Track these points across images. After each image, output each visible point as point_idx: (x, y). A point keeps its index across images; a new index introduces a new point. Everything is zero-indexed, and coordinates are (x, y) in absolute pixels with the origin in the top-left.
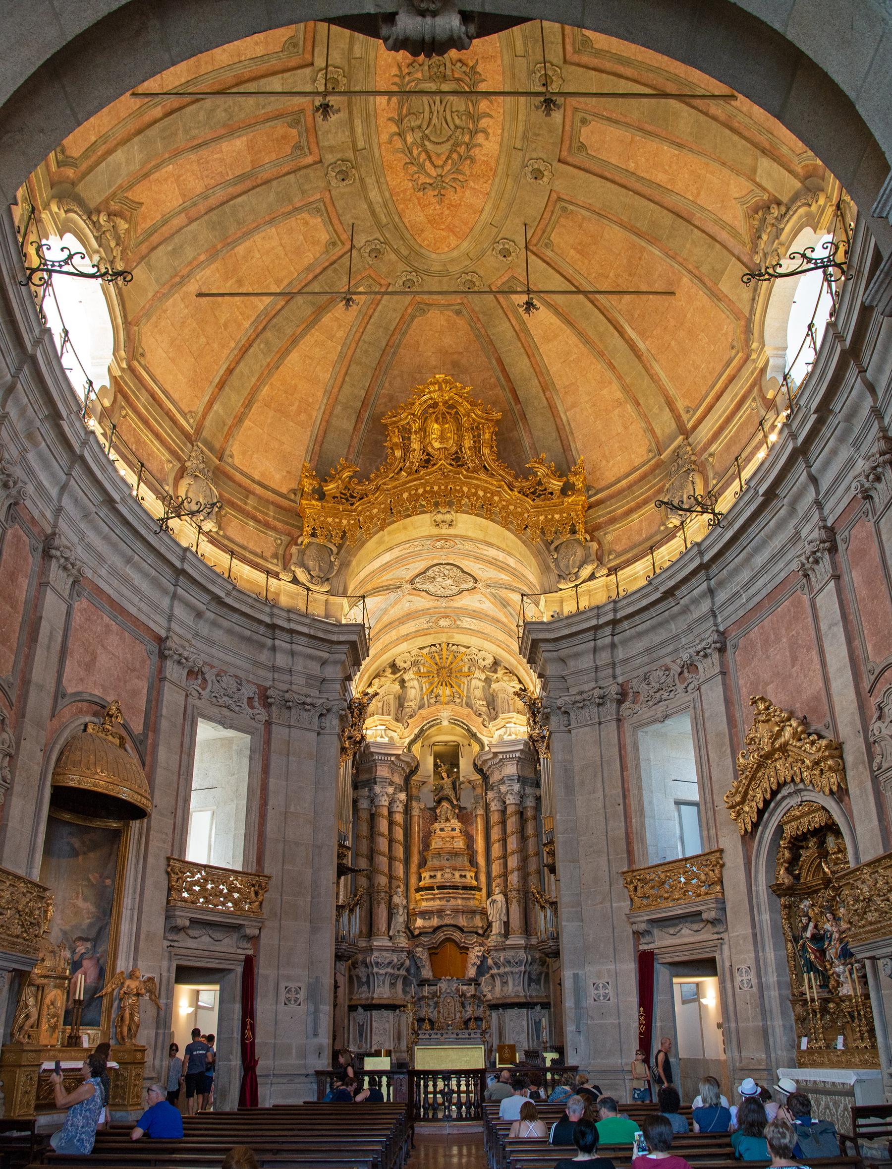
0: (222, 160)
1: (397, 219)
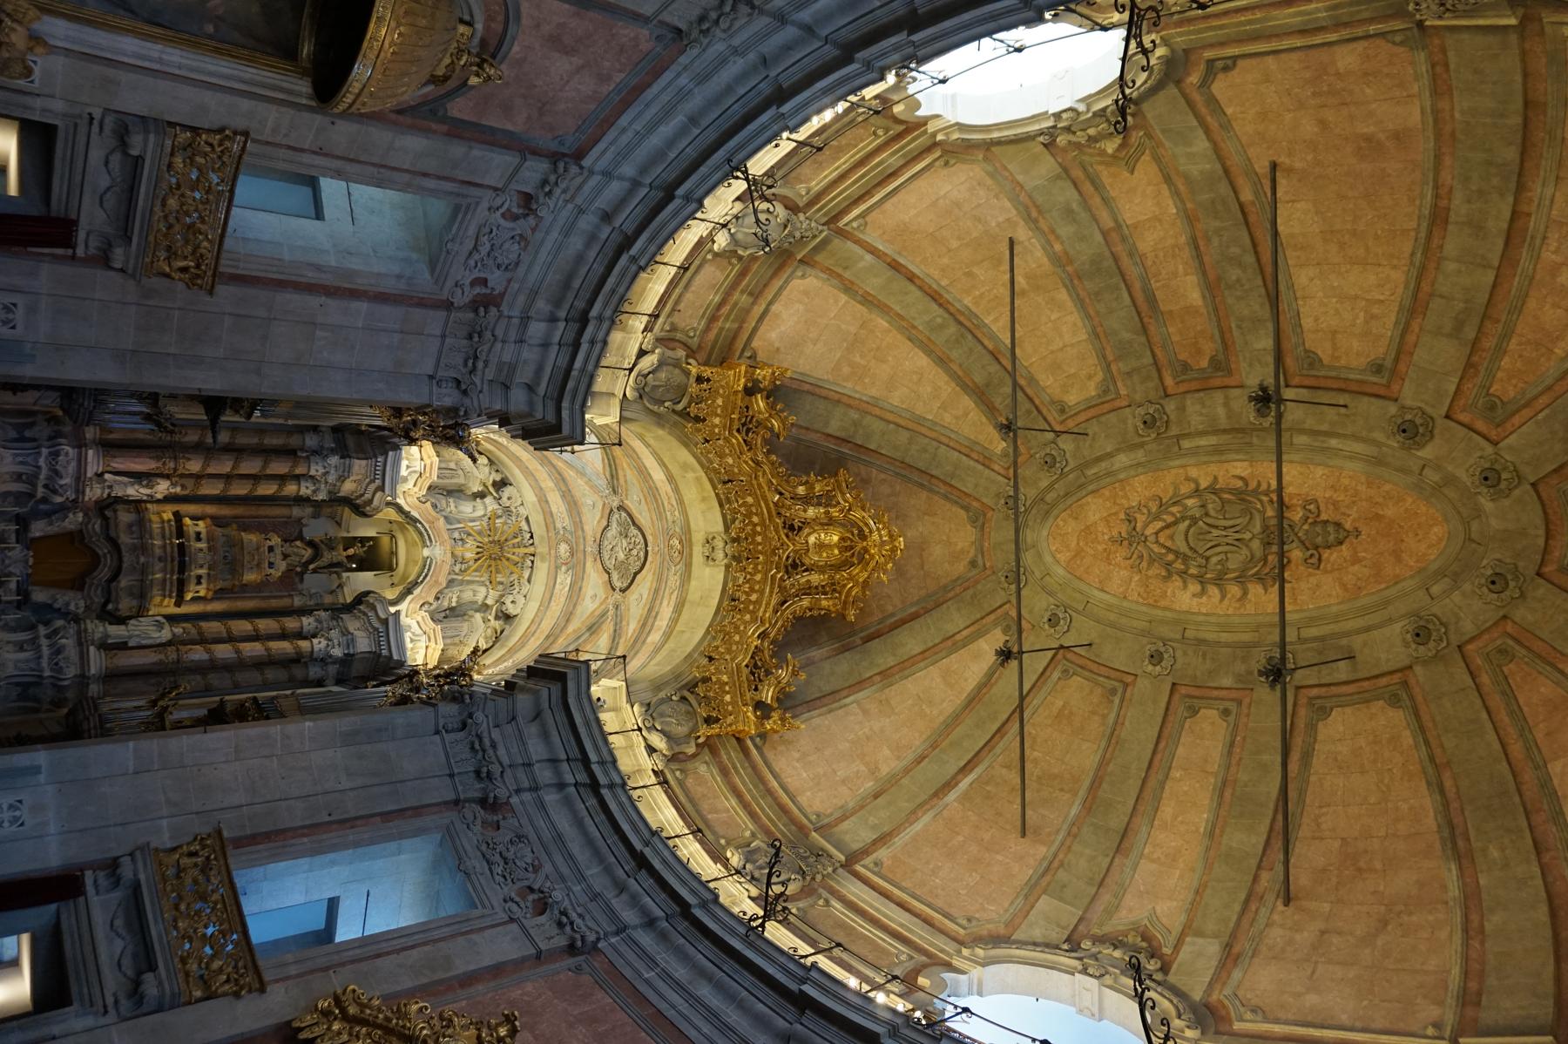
0: (1175, 274)
1: (1091, 488)
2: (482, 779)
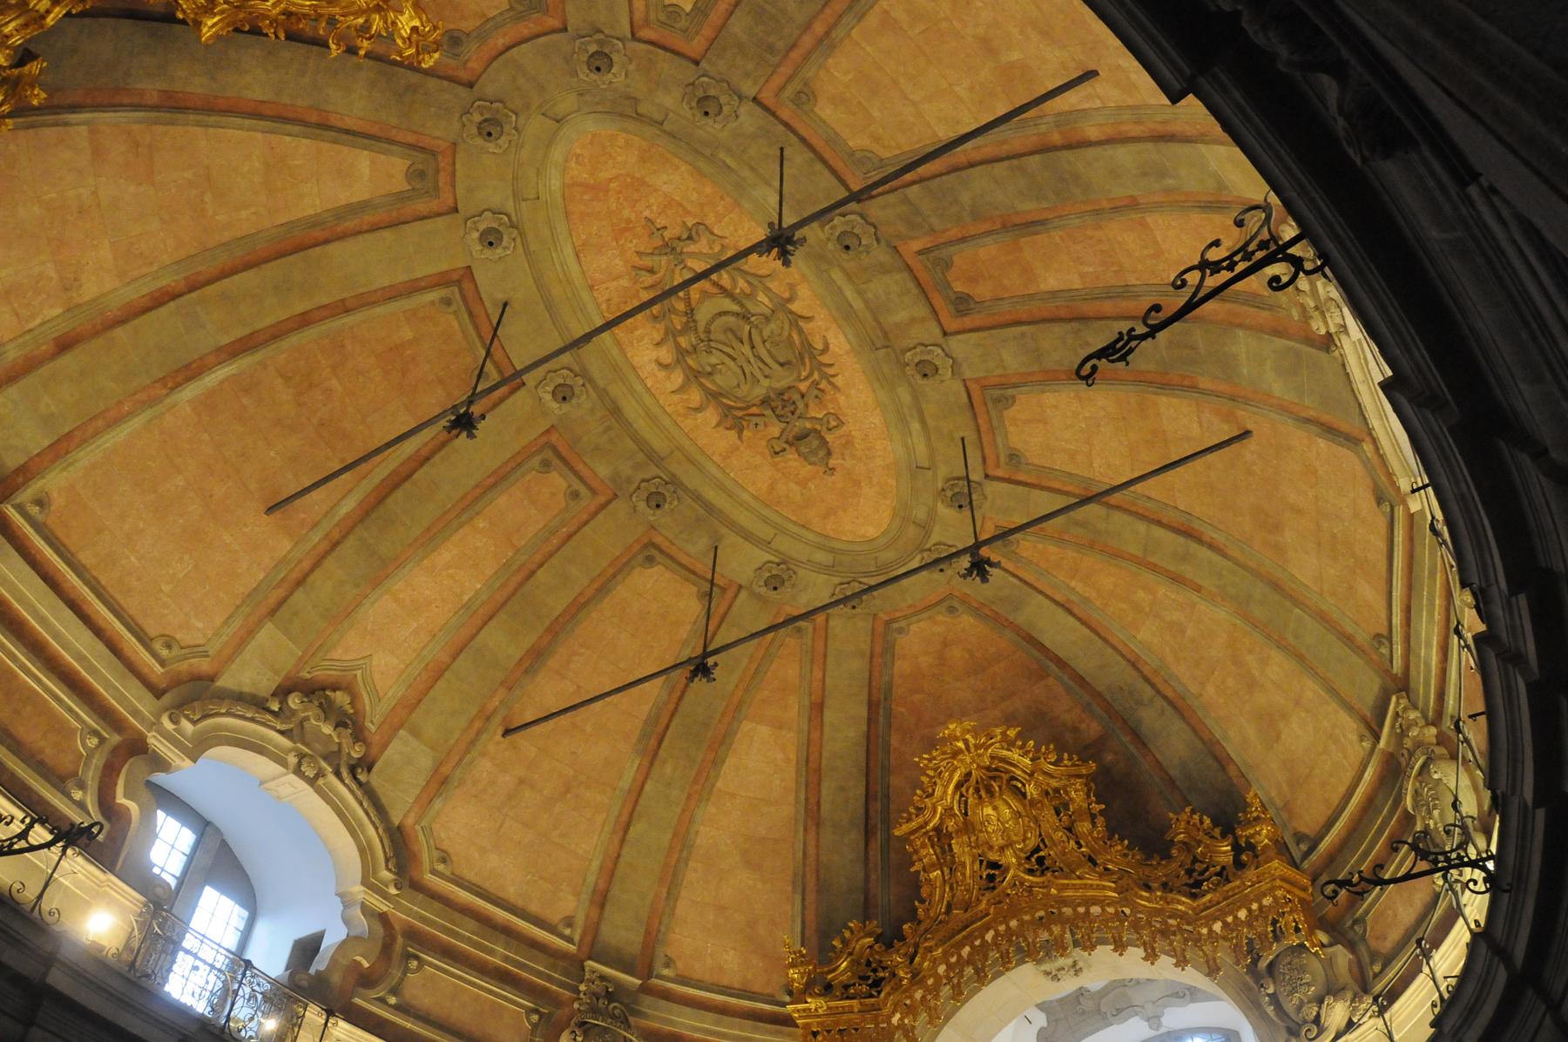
1: (702, 164)
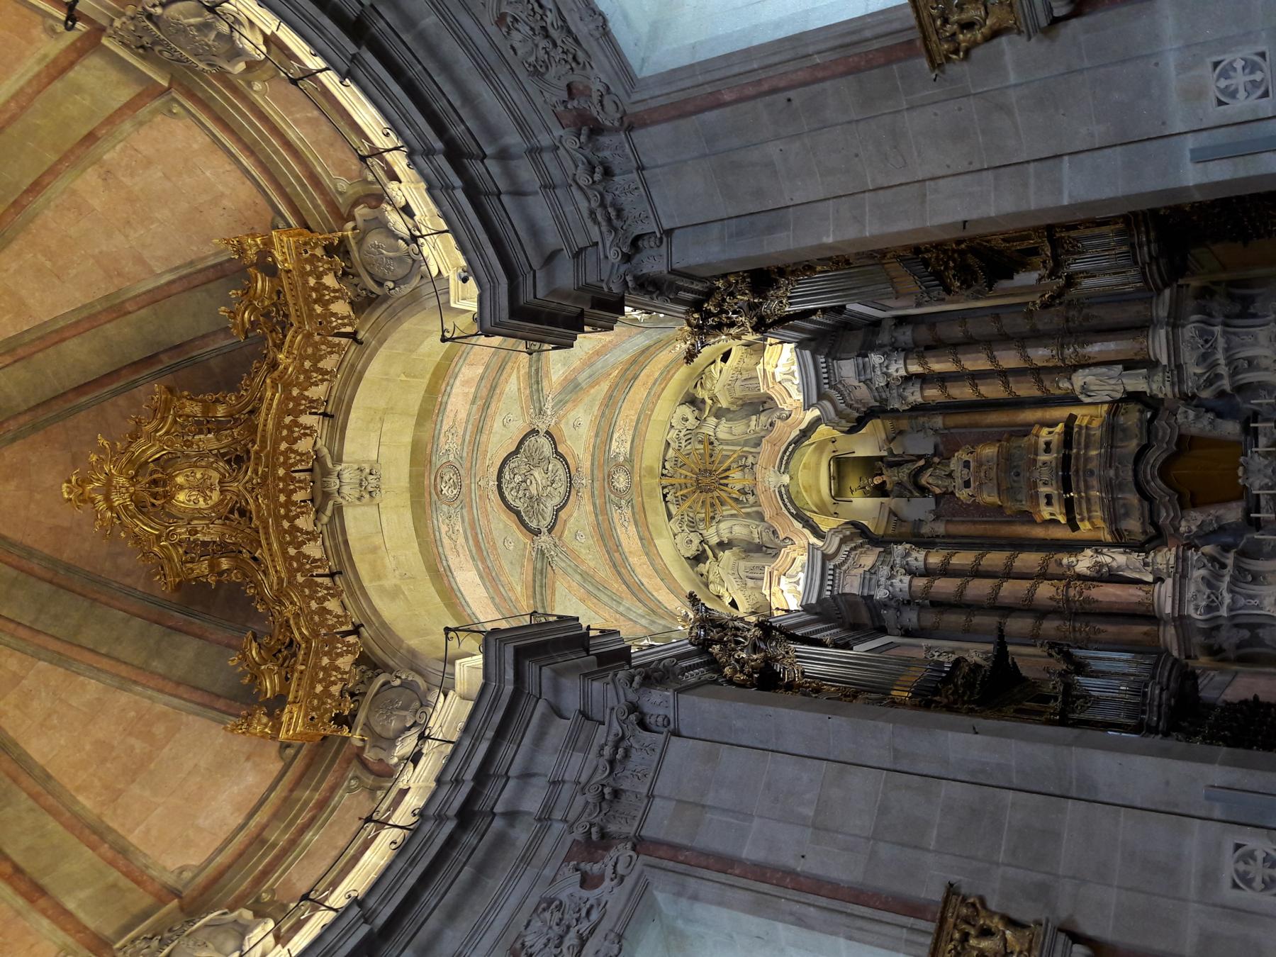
2: (601, 163)
